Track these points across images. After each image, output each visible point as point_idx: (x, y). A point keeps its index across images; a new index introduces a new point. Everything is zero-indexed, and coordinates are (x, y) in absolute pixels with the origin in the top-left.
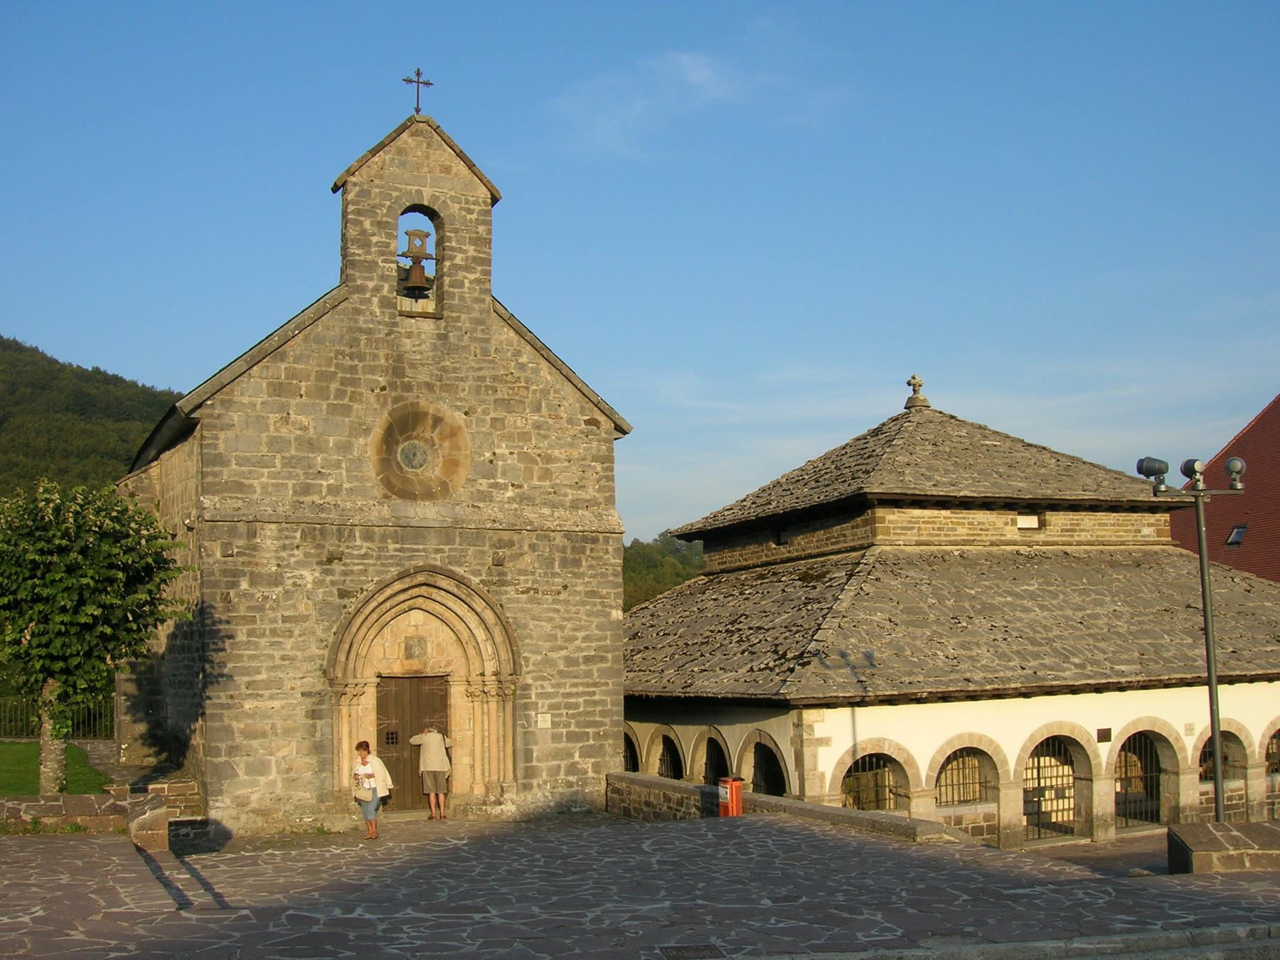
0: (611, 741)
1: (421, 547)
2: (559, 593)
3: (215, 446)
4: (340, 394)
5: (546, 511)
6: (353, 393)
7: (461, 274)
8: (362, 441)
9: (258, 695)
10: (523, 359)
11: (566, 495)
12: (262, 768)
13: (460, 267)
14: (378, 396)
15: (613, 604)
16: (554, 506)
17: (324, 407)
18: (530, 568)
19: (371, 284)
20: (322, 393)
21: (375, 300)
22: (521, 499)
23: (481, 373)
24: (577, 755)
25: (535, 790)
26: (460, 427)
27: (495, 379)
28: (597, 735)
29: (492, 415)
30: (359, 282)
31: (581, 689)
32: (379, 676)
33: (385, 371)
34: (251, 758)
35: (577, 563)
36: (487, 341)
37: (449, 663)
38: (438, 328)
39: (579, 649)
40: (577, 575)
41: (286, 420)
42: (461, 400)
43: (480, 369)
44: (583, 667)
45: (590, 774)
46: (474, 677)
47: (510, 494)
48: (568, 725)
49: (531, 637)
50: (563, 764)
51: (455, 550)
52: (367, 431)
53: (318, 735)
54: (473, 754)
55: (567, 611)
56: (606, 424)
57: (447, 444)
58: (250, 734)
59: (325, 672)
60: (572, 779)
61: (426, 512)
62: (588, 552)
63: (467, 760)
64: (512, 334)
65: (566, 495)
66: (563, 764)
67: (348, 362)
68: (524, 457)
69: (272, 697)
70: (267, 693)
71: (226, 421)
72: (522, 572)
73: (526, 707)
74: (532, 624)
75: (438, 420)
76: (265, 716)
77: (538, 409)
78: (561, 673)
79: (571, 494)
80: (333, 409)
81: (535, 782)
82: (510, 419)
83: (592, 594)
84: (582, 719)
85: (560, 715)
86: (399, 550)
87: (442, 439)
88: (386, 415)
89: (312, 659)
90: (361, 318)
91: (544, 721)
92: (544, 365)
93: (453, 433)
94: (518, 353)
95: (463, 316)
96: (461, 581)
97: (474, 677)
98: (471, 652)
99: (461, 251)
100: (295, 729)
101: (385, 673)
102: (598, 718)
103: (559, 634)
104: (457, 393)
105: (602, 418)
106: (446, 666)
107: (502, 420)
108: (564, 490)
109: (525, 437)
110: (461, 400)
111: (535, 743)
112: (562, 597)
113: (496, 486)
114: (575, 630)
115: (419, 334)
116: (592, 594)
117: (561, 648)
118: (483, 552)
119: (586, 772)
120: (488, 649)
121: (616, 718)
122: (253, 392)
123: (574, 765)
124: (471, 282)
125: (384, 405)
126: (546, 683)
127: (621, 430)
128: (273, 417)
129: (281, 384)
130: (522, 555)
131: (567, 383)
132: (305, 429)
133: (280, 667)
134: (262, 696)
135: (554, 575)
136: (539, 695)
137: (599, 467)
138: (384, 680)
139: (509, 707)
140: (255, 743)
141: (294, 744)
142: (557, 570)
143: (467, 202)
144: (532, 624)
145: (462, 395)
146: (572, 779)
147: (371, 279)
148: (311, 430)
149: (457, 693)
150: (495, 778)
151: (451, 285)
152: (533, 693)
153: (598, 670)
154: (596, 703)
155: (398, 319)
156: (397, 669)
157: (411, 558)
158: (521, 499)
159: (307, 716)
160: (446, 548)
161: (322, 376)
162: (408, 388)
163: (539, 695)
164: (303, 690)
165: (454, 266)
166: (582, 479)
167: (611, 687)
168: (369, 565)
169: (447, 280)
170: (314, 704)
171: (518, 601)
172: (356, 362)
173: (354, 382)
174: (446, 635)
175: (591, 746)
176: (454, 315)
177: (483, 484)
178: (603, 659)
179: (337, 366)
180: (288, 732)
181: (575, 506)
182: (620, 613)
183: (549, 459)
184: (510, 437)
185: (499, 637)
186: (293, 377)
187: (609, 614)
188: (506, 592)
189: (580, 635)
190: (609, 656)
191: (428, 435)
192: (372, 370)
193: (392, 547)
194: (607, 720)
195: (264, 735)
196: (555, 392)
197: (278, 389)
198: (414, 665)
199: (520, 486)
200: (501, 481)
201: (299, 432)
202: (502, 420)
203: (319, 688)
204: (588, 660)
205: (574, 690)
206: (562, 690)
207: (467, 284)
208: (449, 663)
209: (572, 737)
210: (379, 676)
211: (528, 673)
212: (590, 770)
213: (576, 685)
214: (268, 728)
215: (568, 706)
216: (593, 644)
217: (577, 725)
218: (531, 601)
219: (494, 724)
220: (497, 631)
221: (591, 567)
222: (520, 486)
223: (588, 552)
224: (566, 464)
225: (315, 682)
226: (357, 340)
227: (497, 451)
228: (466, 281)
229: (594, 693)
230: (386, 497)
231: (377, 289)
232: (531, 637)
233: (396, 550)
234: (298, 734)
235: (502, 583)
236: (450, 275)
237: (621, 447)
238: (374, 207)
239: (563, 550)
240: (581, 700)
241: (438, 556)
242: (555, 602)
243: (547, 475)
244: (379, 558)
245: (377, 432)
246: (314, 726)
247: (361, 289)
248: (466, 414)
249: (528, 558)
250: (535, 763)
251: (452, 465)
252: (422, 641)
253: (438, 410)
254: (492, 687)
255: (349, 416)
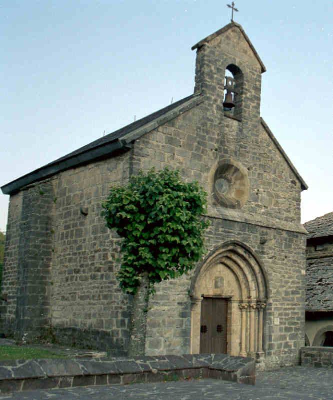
0: (300, 332)
1: (232, 231)
2: (284, 260)
3: (139, 164)
4: (198, 149)
5: (277, 220)
6: (203, 149)
7: (249, 102)
8: (205, 174)
9: (157, 303)
10: (270, 148)
11: (283, 214)
12: (156, 344)
13: (248, 99)
14: (214, 153)
15: (302, 266)
16: (279, 219)
17: (190, 154)
18: (273, 247)
19: (213, 98)
20: (189, 146)
21: (215, 106)
22: (268, 213)
23: (256, 151)
24: (288, 338)
25: (272, 355)
26: (246, 175)
27: (260, 154)
28: (295, 328)
29: (258, 171)
30: (208, 95)
31: (290, 307)
32: (202, 296)
33: (217, 141)
34: (152, 339)
35: (290, 246)
36: (257, 136)
37: (232, 291)
38: (239, 125)
39: (290, 287)
40: (290, 252)
41: (173, 157)
42: (247, 162)
43: (254, 149)
44: (291, 296)
45: (293, 348)
46: (245, 298)
47: (263, 210)
48: (285, 324)
49: (272, 280)
50: (283, 342)
51: (245, 234)
52: (208, 169)
53: (184, 326)
54: (241, 339)
55: (286, 269)
56: (298, 184)
57: (238, 182)
58: (154, 325)
59: (189, 292)
60: (286, 350)
61: (232, 214)
62: (294, 241)
63: (238, 341)
64: (267, 135)
65: (283, 214)
66: (283, 342)
67: (202, 134)
68: (269, 194)
69: (164, 305)
70: (162, 302)
71: (144, 152)
72: (270, 248)
73: (270, 314)
74: (274, 274)
75: (237, 170)
76: (160, 315)
77: (275, 172)
78: (283, 298)
79: (285, 214)
80: (194, 156)
81: (272, 351)
82: (265, 174)
83: (295, 261)
84: (290, 320)
85: (282, 319)
86: (224, 231)
87: (236, 179)
88: (216, 163)
89: (184, 285)
90: (208, 113)
91: (277, 321)
92: (278, 152)
93: (242, 177)
94: (268, 145)
95: (249, 123)
96: (247, 250)
97: (245, 298)
98: (243, 286)
99: (250, 92)
100: (173, 323)
101: (206, 294)
102: (296, 321)
103: (283, 280)
104: (245, 158)
105: (297, 181)
106: (231, 293)
107: (262, 174)
108: (283, 212)
109: (269, 184)
110: (247, 162)
111: (273, 332)
112: (284, 262)
113: (258, 206)
114: (289, 278)
115: (232, 126)
116: (295, 261)
117: (283, 286)
118: (256, 237)
119: (291, 347)
120: (252, 285)
121: (302, 321)
122: (158, 139)
123: (287, 343)
124: (253, 107)
125: (216, 158)
126: (277, 303)
127: (304, 187)
128: (167, 155)
129: (172, 138)
130: (271, 240)
131: (285, 162)
132: (181, 163)
133: (169, 288)
134: (159, 303)
135: (283, 251)
136: (276, 308)
137: (295, 203)
138: (206, 298)
139: (261, 314)
140: (155, 330)
141: (173, 330)
142: (283, 249)
143: (253, 69)
144: (274, 274)
145: (247, 160)
146: (286, 350)
147: (213, 95)
148: (184, 165)
149: (235, 306)
150: (252, 349)
151: (245, 107)
152: (273, 307)
153: (297, 298)
154: (296, 313)
155: (224, 117)
156: (211, 293)
157: (228, 236)
158: (268, 213)
159: (179, 315)
160: (242, 233)
161: (191, 139)
162: (226, 152)
163: (276, 308)
164: (178, 301)
165: (246, 98)
166: (289, 207)
167: (301, 306)
168: (211, 238)
169: (243, 103)
170: (183, 308)
171: (268, 262)
172: (205, 134)
173: (204, 144)
174: (231, 277)
175: (293, 334)
176: (245, 121)
177: (253, 204)
178: (298, 293)
179: (197, 134)
180: (171, 324)
181: (286, 219)
182: (304, 271)
183: (278, 196)
184: (264, 183)
185: (260, 280)
186: (178, 135)
187: (300, 272)
188: (264, 258)
189: (291, 280)
190: (300, 291)
191: (229, 177)
192: (212, 139)
193: (221, 229)
194: (299, 322)
195: (159, 325)
196: (281, 166)
197: (170, 141)
198: (218, 291)
199: (267, 208)
200: (260, 203)
201: (178, 165)
202: (262, 174)
203: (186, 300)
204: (293, 293)
205: (288, 307)
206: (283, 307)
207: (251, 108)
208: (232, 291)
209: (287, 329)
210: (202, 296)
211: (272, 297)
212: (292, 346)
213: (288, 304)
214: (161, 321)
215: (287, 315)
216: (295, 285)
217: (288, 324)
218: (274, 263)
219: (253, 322)
220: (259, 276)
221: (295, 249)
222: (267, 208)
223: (294, 241)
224: (284, 200)
225: (184, 298)
226: (206, 123)
227: (260, 190)
228: (251, 106)
229: (294, 309)
230: (214, 204)
231: (216, 100)
232: (272, 280)
233: (222, 231)
234: (174, 325)
235: (263, 253)
236: (245, 101)
237: (304, 194)
238: (216, 60)
239: (286, 240)
240: (290, 312)
241: (239, 236)
242: (283, 264)
243: (277, 203)
244: (215, 234)
245: (212, 171)
246: (183, 321)
247: (208, 98)
248: (249, 169)
249: (273, 241)
250: (272, 342)
251: (240, 193)
252: (222, 279)
253: (238, 165)
254: (253, 304)
255: (200, 161)
